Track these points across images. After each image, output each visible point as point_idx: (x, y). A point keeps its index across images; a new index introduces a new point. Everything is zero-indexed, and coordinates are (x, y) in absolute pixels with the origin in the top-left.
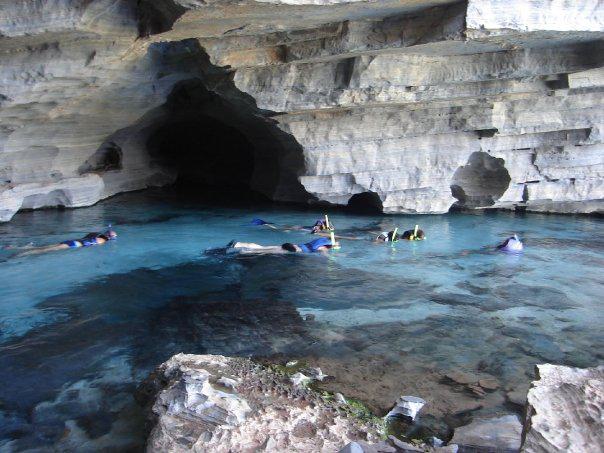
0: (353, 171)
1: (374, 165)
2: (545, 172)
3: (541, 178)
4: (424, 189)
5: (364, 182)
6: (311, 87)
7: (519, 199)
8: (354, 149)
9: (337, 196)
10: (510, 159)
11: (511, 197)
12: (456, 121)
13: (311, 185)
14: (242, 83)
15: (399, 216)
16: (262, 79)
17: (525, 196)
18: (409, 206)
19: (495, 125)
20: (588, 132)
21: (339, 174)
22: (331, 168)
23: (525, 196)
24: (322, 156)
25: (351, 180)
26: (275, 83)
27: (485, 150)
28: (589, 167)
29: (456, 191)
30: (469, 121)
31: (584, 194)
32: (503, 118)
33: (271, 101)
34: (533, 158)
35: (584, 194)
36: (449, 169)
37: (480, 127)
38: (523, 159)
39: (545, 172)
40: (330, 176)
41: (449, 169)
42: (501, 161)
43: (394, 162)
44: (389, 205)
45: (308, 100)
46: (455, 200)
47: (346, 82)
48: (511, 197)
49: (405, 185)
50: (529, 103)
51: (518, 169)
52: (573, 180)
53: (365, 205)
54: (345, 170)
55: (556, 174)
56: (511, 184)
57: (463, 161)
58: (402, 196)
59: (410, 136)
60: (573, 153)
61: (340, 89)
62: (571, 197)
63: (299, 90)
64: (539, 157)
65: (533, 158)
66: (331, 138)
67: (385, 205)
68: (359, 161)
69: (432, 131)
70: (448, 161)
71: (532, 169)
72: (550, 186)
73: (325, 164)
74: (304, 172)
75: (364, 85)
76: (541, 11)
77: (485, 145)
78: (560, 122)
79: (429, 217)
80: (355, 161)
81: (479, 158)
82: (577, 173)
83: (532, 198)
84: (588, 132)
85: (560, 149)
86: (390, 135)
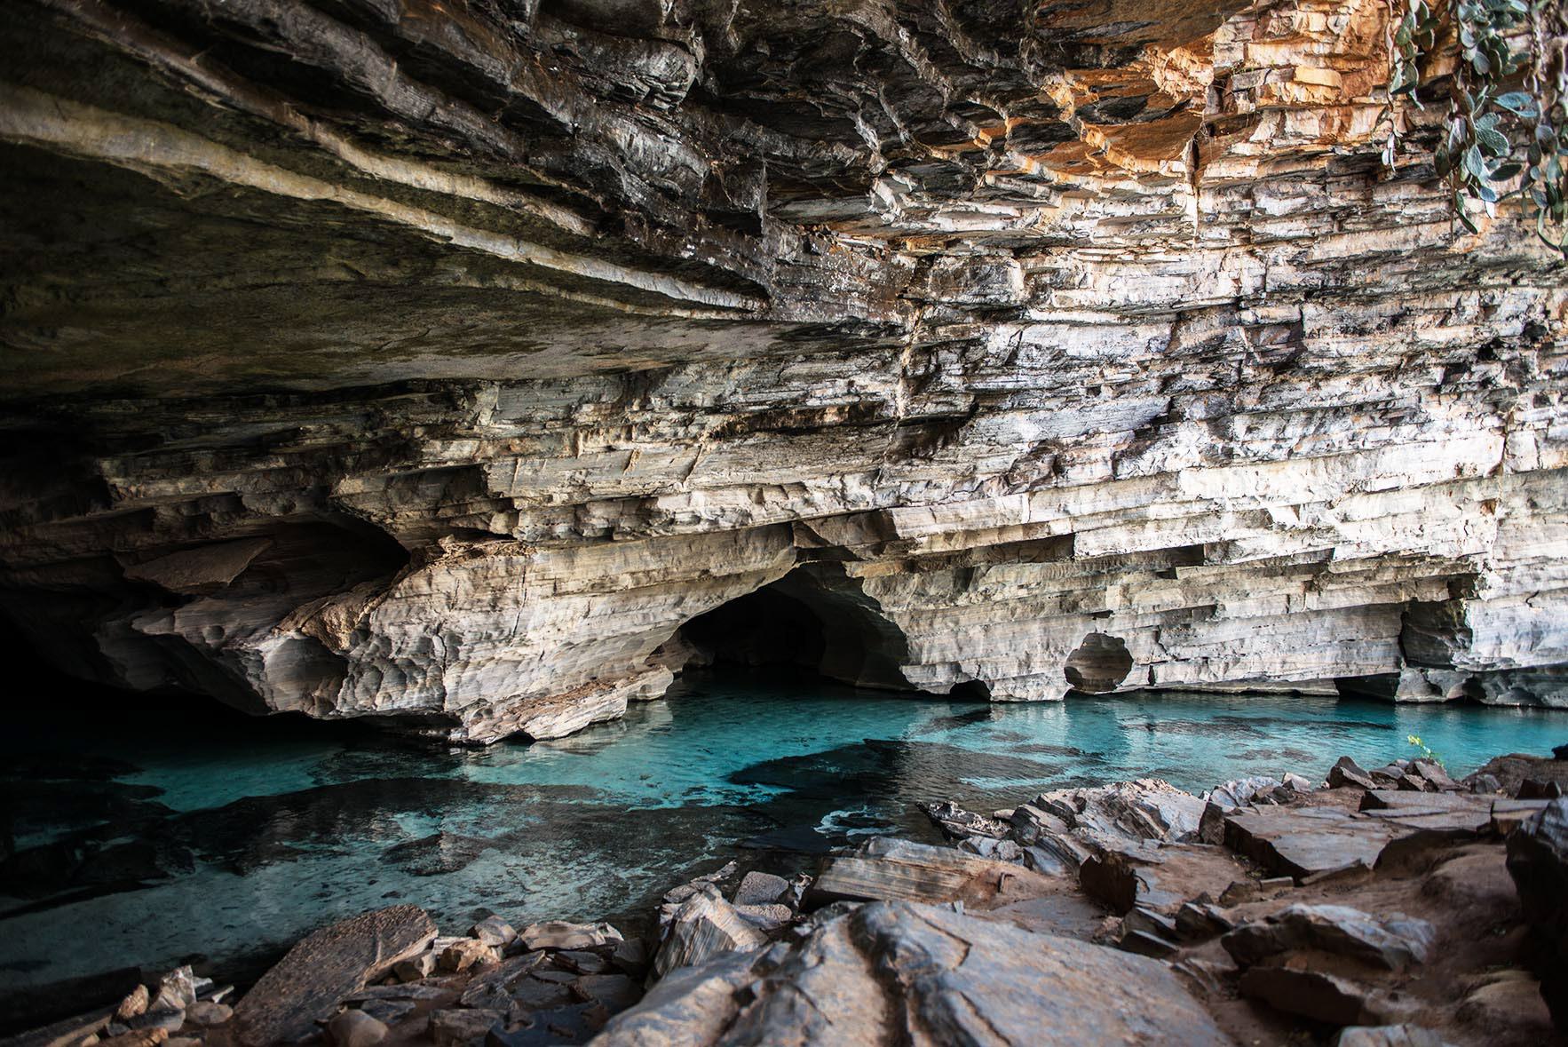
0: (959, 658)
1: (980, 651)
2: (1172, 651)
3: (1169, 658)
4: (1036, 676)
5: (970, 668)
6: (932, 591)
7: (1145, 682)
8: (960, 636)
9: (940, 685)
10: (1131, 637)
11: (1135, 678)
12: (1068, 606)
13: (913, 674)
14: (869, 589)
15: (1006, 703)
16: (887, 585)
17: (1152, 679)
18: (1020, 694)
19: (1108, 608)
20: (1213, 608)
21: (943, 663)
22: (936, 657)
23: (1152, 679)
24: (927, 645)
25: (956, 668)
26: (899, 589)
27: (1100, 631)
28: (1223, 644)
29: (1070, 674)
30: (1082, 604)
31: (1220, 674)
32: (1119, 598)
33: (894, 604)
34: (1157, 636)
35: (1220, 674)
36: (1062, 653)
37: (1094, 610)
38: (1145, 639)
39: (1172, 651)
40: (934, 665)
41: (1062, 653)
42: (1122, 641)
43: (1002, 647)
44: (997, 692)
45: (928, 601)
46: (1070, 686)
47: (965, 587)
48: (1135, 678)
49: (1014, 672)
50: (1143, 585)
51: (1142, 649)
52: (1206, 658)
53: (971, 698)
54: (950, 658)
55: (1185, 652)
56: (1134, 666)
57: (1077, 645)
58: (1011, 684)
59: (1018, 621)
60: (1202, 630)
61: (960, 593)
62: (1204, 677)
63: (920, 594)
64: (1164, 637)
65: (1157, 636)
66: (936, 626)
67: (993, 694)
68: (966, 649)
69: (1042, 615)
70: (1060, 646)
71: (1156, 648)
72: (1179, 666)
73: (930, 652)
74: (907, 662)
75: (981, 589)
76: (1136, 537)
77: (1100, 626)
78: (1180, 598)
79: (1043, 704)
80: (961, 649)
81: (1095, 639)
82: (1210, 651)
83: (1160, 680)
84: (1213, 608)
85: (1187, 626)
86: (997, 620)
